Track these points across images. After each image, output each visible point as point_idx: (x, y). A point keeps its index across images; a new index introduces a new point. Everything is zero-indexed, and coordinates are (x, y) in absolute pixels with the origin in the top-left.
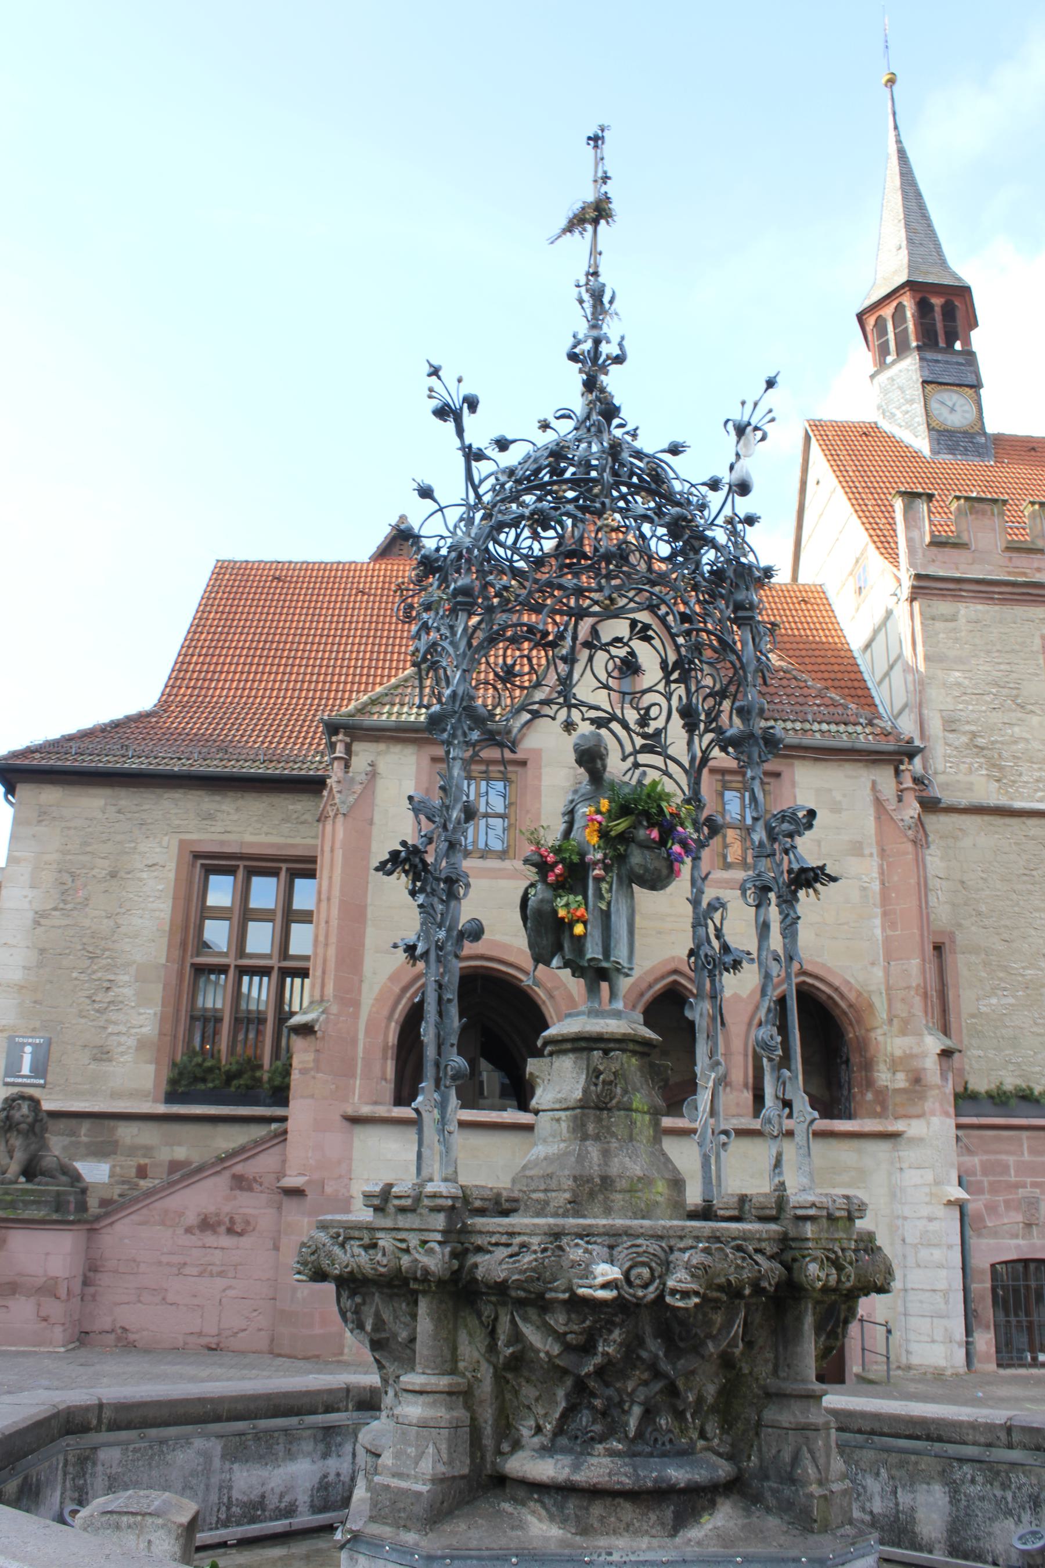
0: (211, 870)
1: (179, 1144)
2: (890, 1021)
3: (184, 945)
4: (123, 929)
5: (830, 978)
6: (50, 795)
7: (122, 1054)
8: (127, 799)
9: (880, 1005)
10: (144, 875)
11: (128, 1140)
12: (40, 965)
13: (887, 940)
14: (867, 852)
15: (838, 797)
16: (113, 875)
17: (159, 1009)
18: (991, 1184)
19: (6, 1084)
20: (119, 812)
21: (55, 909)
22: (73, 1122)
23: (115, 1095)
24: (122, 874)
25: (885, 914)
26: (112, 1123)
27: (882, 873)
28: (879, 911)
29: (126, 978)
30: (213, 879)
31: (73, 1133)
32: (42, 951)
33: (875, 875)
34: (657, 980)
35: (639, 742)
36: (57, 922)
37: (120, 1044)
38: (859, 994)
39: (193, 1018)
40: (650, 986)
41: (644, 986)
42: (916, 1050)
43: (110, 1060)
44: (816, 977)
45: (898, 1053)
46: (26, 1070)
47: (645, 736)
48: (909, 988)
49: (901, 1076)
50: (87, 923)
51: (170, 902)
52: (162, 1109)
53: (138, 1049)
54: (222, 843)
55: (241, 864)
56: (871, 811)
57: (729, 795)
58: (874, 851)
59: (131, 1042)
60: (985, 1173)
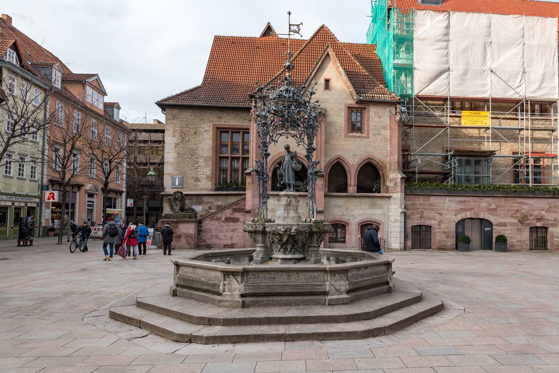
0: (221, 132)
1: (219, 201)
2: (390, 170)
3: (216, 152)
4: (199, 148)
5: (376, 160)
6: (175, 112)
7: (202, 179)
8: (197, 113)
9: (388, 166)
10: (204, 133)
11: (206, 200)
12: (178, 157)
13: (390, 150)
14: (387, 128)
15: (380, 114)
16: (195, 133)
17: (211, 168)
18: (412, 208)
19: (172, 188)
20: (195, 116)
21: (180, 143)
22: (191, 196)
23: (201, 190)
24: (198, 133)
25: (390, 144)
26: (201, 196)
27: (390, 134)
28: (389, 143)
29: (202, 160)
30: (223, 134)
31: (192, 199)
32: (178, 154)
33: (388, 134)
34: (334, 161)
35: (299, 140)
36: (181, 146)
37: (201, 177)
38: (383, 163)
39: (220, 170)
40: (333, 162)
41: (331, 162)
42: (396, 177)
43: (199, 181)
44: (373, 159)
45: (392, 178)
46: (177, 184)
47: (300, 139)
48: (395, 162)
49: (392, 183)
50: (190, 146)
51: (212, 141)
52: (214, 193)
53: (206, 178)
54: (224, 125)
55: (230, 130)
56: (389, 118)
57: (353, 114)
58: (389, 128)
59: (204, 176)
60: (411, 206)
